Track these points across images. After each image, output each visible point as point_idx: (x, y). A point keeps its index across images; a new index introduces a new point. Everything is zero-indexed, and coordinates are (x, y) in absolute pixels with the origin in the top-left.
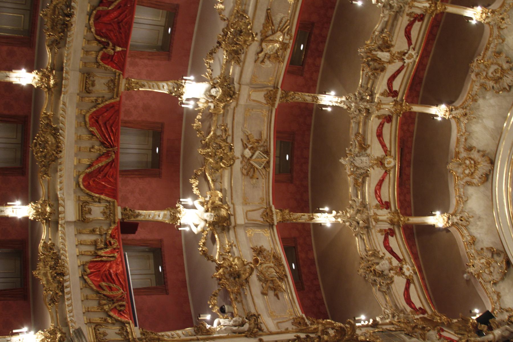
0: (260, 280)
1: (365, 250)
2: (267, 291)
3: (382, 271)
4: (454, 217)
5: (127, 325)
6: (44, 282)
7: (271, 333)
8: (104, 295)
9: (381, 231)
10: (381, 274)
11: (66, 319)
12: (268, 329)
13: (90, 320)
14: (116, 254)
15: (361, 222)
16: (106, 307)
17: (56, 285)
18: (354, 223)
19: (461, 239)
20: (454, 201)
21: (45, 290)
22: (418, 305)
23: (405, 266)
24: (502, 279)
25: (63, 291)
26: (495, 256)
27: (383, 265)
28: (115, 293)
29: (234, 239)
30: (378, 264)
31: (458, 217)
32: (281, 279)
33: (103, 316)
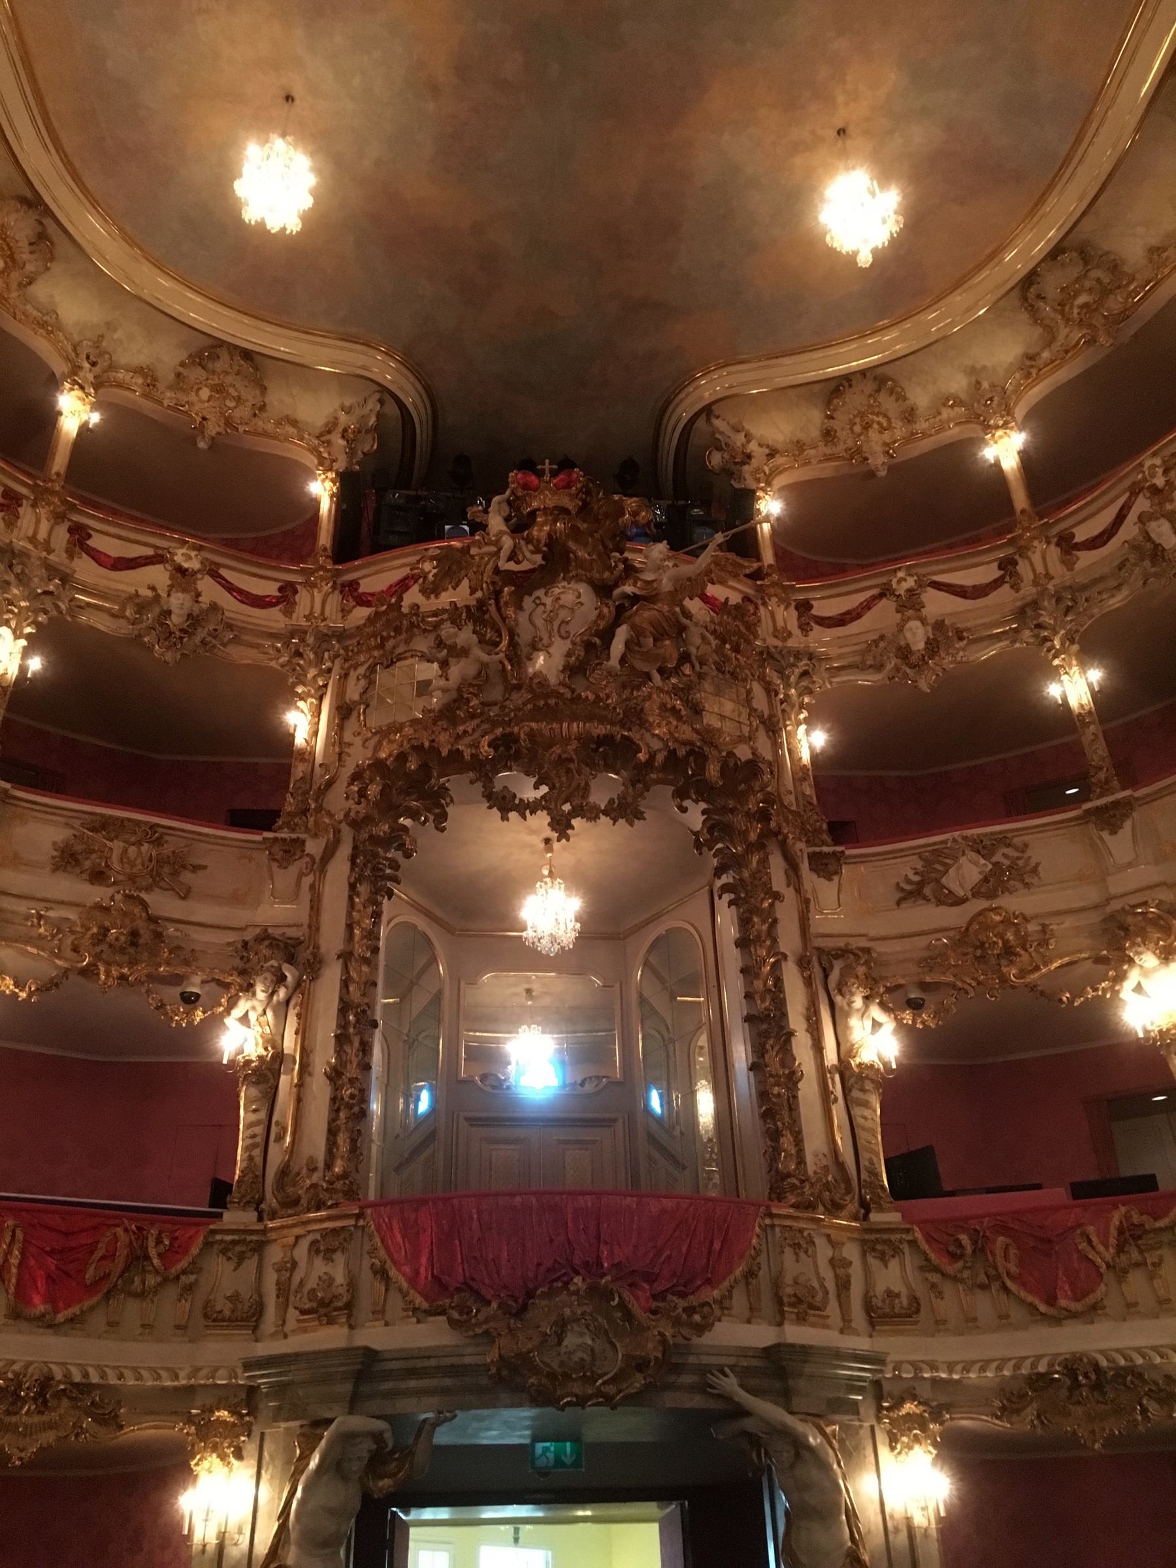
0: (148, 889)
1: (114, 616)
2: (182, 883)
3: (189, 616)
4: (81, 374)
5: (218, 1237)
6: (49, 1437)
7: (314, 927)
8: (121, 1276)
9: (71, 555)
10: (195, 621)
11: (176, 1389)
12: (298, 926)
13: (178, 1327)
14: (10, 1222)
15: (51, 588)
16: (151, 1280)
17: (65, 1402)
18: (48, 603)
19: (135, 397)
20: (41, 345)
21: (77, 1435)
22: (269, 589)
23: (178, 558)
24: (264, 389)
25: (85, 1388)
26: (210, 365)
27: (178, 603)
28: (122, 1253)
29: (32, 904)
30: (169, 613)
31: (86, 365)
32: (158, 842)
33: (172, 1292)
